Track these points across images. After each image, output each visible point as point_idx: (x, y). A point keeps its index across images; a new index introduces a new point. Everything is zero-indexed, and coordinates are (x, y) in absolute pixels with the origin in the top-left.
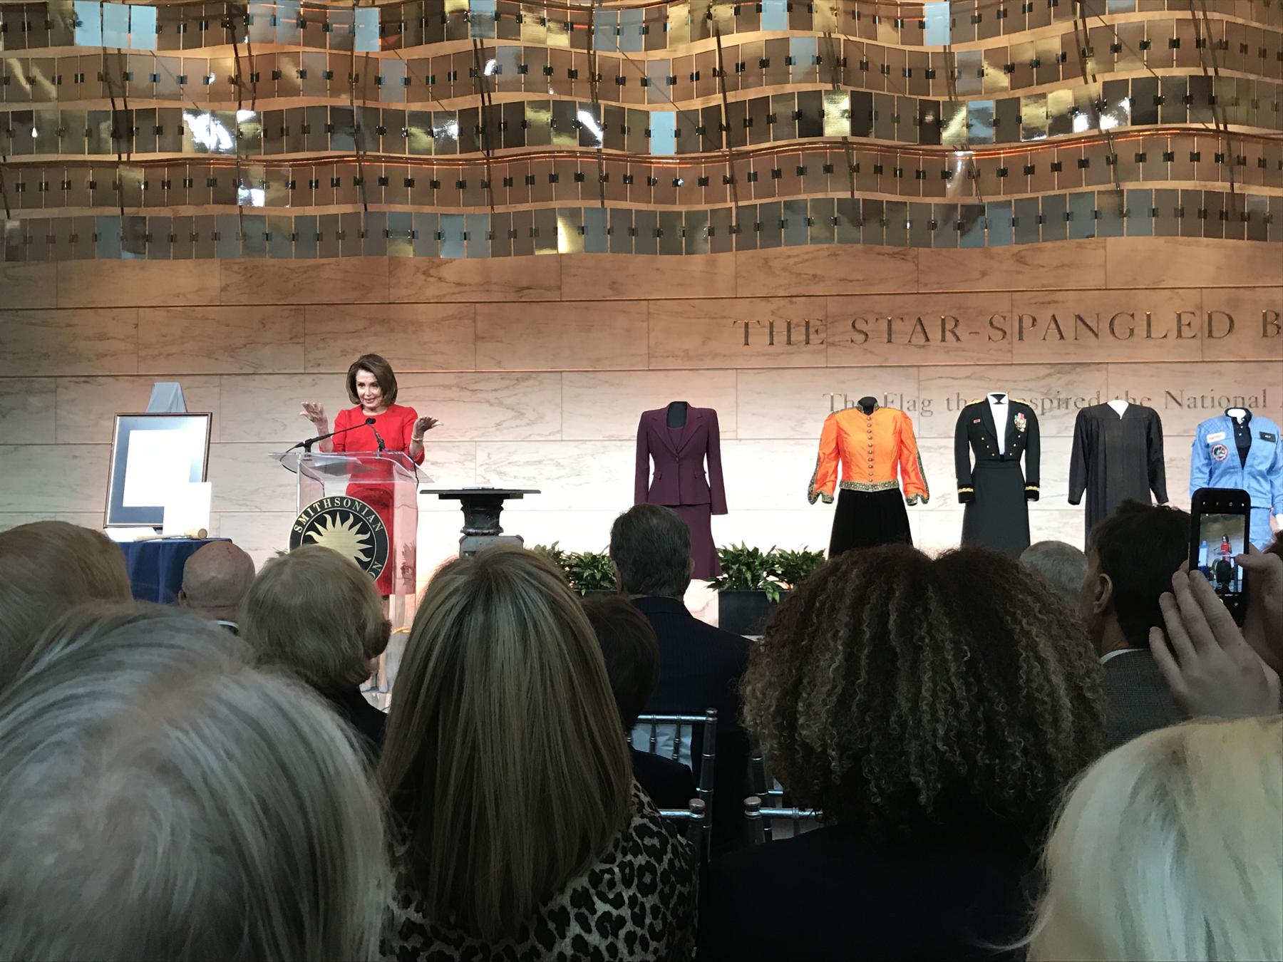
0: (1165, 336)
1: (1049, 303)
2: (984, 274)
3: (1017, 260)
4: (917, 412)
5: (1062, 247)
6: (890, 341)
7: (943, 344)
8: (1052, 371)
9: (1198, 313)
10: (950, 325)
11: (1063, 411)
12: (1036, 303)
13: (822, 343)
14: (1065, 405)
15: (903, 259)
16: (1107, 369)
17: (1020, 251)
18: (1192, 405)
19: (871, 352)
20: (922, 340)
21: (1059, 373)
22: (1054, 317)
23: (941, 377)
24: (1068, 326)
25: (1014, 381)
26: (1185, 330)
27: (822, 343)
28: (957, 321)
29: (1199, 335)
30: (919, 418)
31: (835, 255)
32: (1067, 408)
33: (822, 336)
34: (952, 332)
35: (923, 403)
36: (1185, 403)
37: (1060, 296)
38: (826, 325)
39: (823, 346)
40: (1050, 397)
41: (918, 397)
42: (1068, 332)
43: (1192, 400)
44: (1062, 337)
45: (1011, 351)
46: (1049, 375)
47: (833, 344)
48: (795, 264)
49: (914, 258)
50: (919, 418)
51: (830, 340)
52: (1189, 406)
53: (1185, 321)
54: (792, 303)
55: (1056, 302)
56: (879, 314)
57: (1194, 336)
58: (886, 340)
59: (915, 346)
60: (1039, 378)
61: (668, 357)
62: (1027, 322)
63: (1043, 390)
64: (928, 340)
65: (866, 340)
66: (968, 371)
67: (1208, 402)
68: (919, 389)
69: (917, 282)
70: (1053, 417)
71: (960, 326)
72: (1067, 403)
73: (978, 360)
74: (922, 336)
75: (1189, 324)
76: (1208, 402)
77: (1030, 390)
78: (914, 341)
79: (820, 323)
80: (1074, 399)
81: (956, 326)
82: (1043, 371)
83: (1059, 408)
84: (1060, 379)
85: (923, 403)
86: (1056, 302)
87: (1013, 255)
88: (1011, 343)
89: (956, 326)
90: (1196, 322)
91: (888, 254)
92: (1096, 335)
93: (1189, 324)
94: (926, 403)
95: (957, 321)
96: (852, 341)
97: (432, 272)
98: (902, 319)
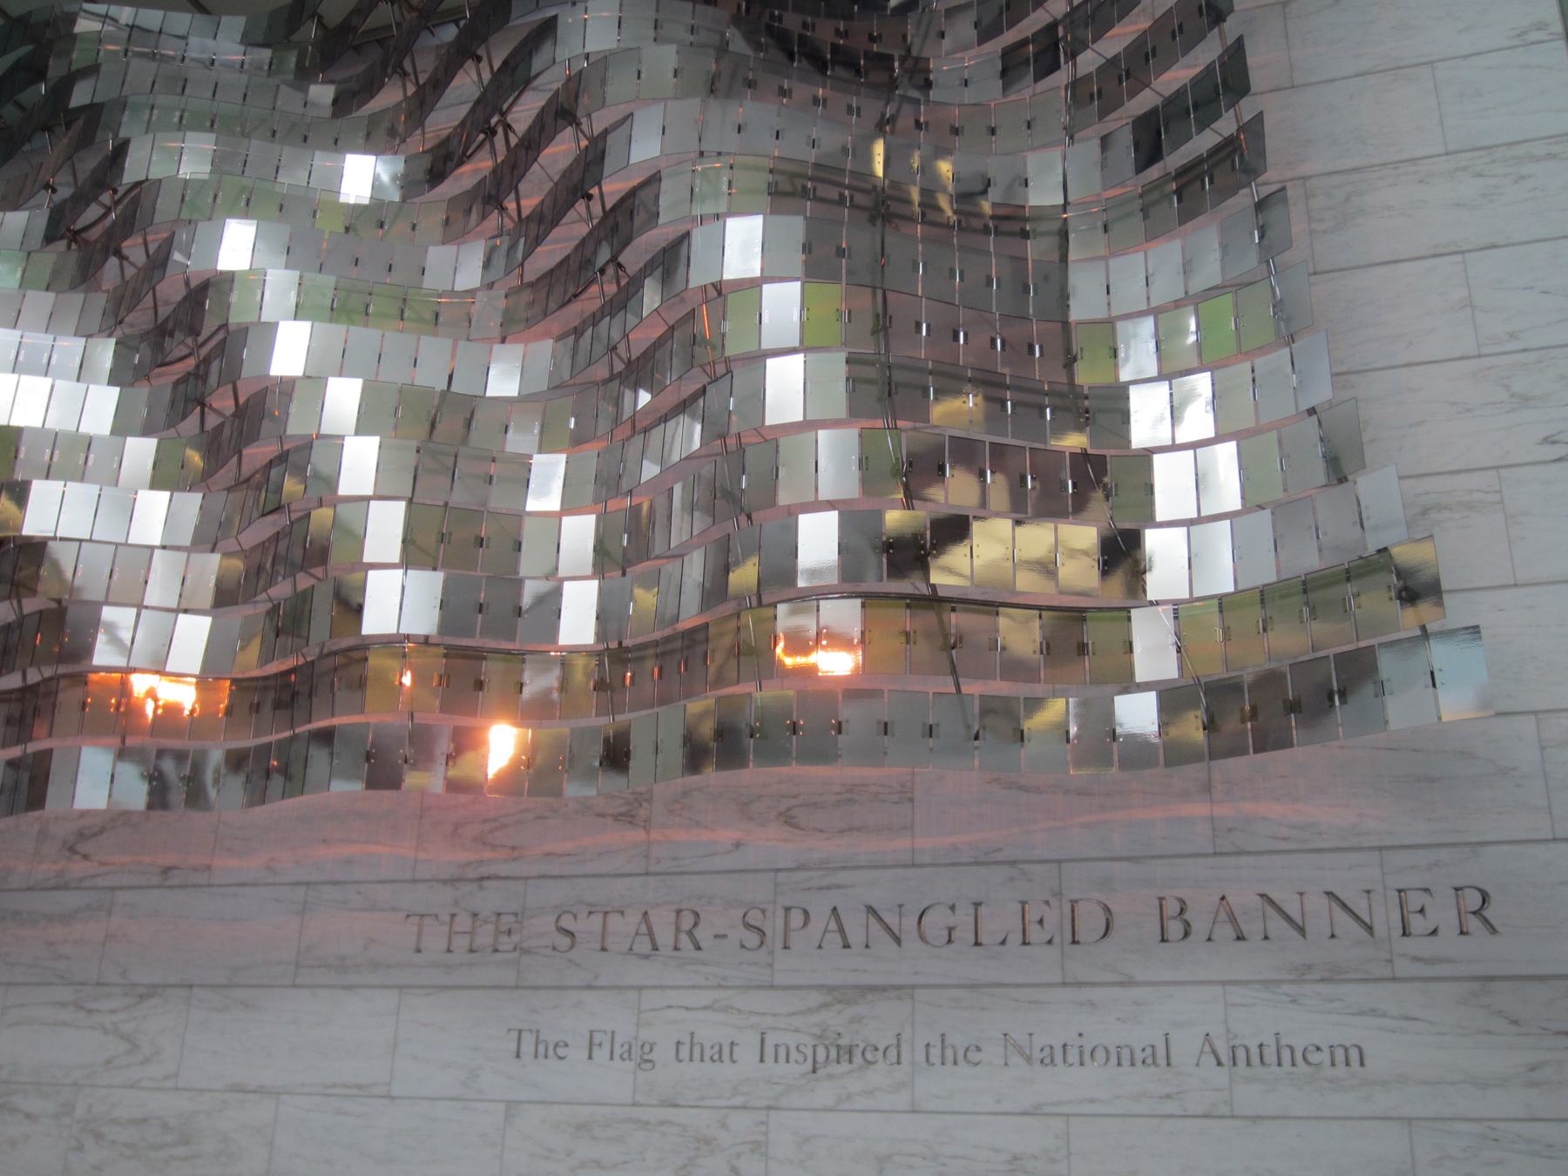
0: (1003, 943)
1: (829, 888)
2: (738, 845)
3: (786, 822)
4: (633, 1062)
5: (850, 800)
6: (604, 949)
7: (677, 954)
8: (829, 999)
9: (1054, 902)
10: (687, 922)
11: (845, 1066)
12: (809, 889)
13: (515, 949)
14: (847, 1057)
15: (631, 823)
16: (912, 998)
17: (789, 809)
18: (1047, 1061)
19: (578, 965)
20: (644, 946)
21: (840, 1002)
22: (835, 909)
23: (670, 1007)
24: (855, 924)
25: (774, 1015)
26: (1035, 934)
27: (515, 949)
28: (697, 915)
29: (1057, 940)
30: (635, 1073)
31: (541, 818)
32: (850, 1062)
33: (515, 938)
34: (690, 933)
35: (642, 1046)
36: (1037, 1055)
37: (843, 877)
38: (521, 923)
39: (516, 954)
40: (826, 1042)
41: (636, 1039)
42: (856, 936)
43: (1047, 1050)
44: (847, 946)
45: (771, 965)
46: (826, 1006)
47: (527, 951)
48: (492, 831)
49: (645, 821)
50: (635, 1073)
51: (525, 945)
52: (1042, 1061)
53: (1032, 916)
54: (481, 888)
55: (838, 887)
56: (589, 904)
57: (1050, 942)
58: (599, 946)
59: (637, 955)
60: (810, 1011)
61: (320, 966)
62: (796, 919)
63: (817, 1031)
64: (655, 948)
65: (572, 947)
66: (706, 997)
67: (1073, 1056)
68: (638, 1025)
69: (646, 857)
70: (830, 1077)
71: (701, 926)
72: (850, 1053)
73: (724, 978)
74: (647, 939)
75: (1041, 922)
76: (1073, 1056)
77: (797, 1030)
78: (636, 949)
79: (512, 918)
80: (862, 1046)
81: (696, 924)
82: (815, 999)
83: (838, 1062)
84: (840, 1012)
85: (642, 1046)
86: (838, 887)
87: (780, 814)
88: (772, 953)
89: (696, 924)
90: (1051, 918)
91: (612, 816)
92: (898, 940)
93: (1041, 922)
94: (647, 1048)
95: (697, 915)
96: (554, 948)
97: (79, 848)
98: (622, 913)
